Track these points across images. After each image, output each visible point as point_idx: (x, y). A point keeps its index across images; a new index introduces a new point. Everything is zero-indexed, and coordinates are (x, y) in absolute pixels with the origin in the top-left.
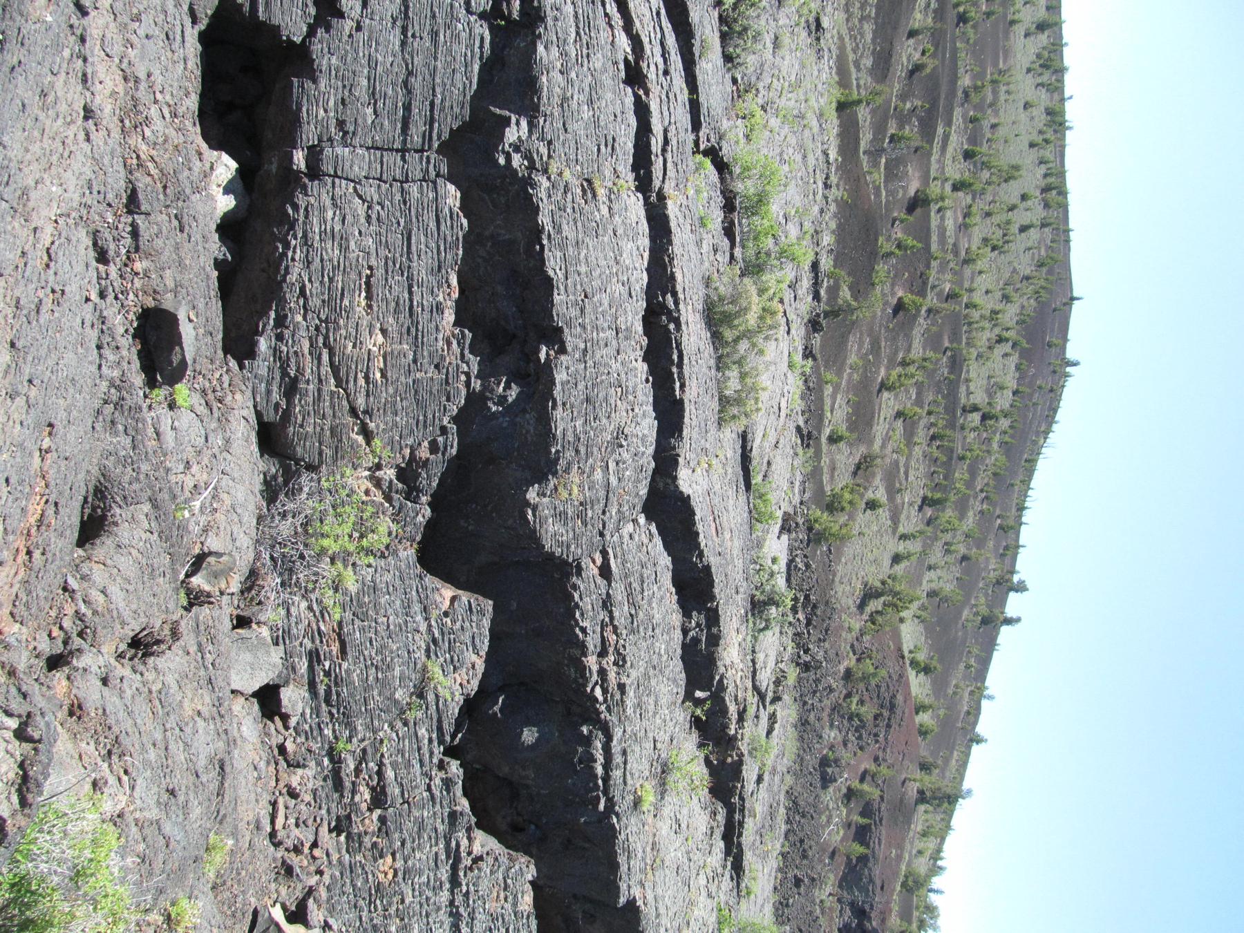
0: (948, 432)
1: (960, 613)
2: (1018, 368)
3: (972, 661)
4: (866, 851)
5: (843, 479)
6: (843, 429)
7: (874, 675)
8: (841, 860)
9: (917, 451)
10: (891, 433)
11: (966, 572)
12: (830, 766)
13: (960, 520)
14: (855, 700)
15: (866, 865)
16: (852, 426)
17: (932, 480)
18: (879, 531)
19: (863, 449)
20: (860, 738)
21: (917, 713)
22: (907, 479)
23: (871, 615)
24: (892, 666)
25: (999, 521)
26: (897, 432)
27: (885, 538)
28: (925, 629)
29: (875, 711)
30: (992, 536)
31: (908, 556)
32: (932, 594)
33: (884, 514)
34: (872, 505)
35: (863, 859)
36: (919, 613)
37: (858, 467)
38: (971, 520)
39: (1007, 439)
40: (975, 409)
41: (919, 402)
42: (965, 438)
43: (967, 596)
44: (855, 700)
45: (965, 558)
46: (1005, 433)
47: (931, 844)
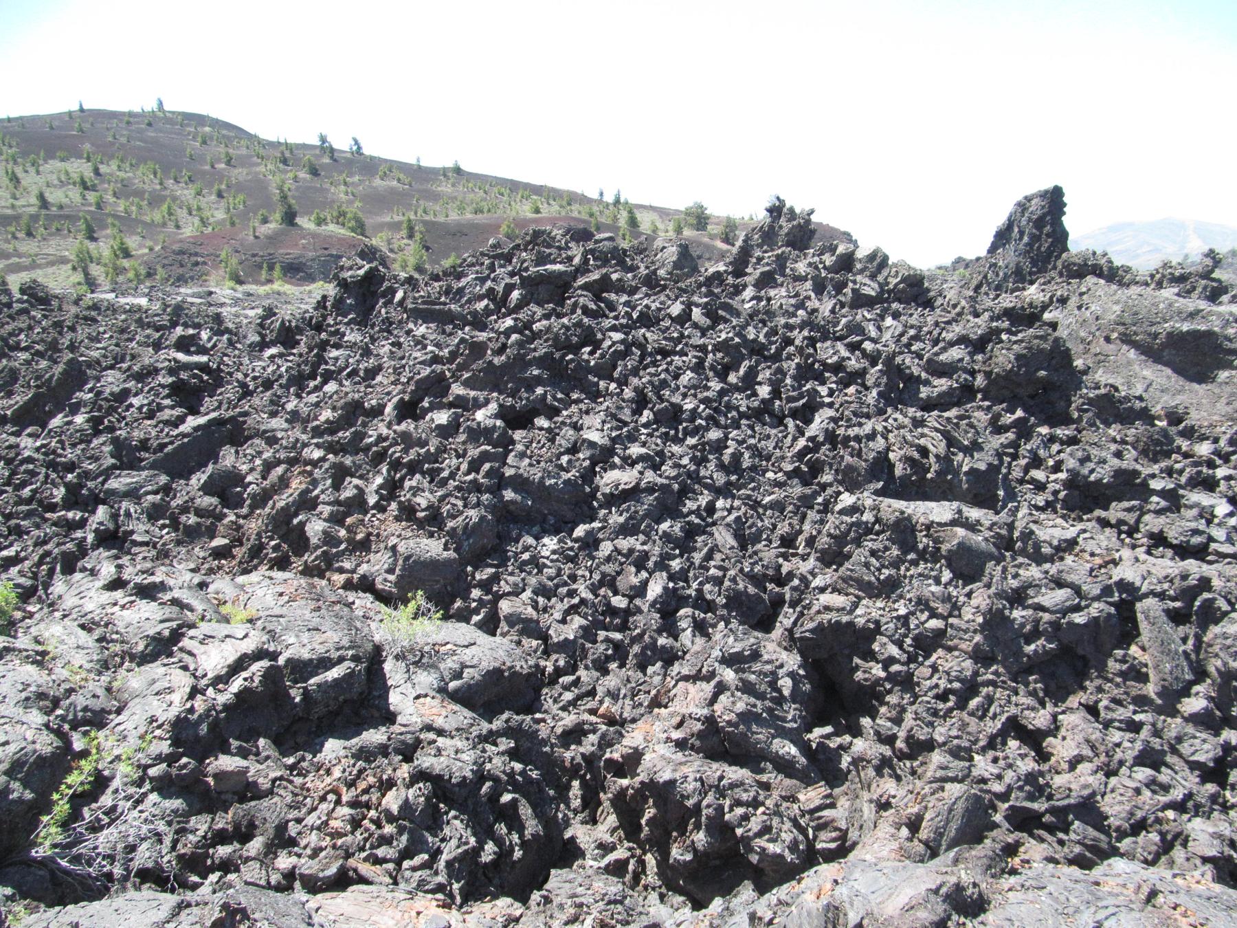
2: (62, 160)
38: (186, 192)
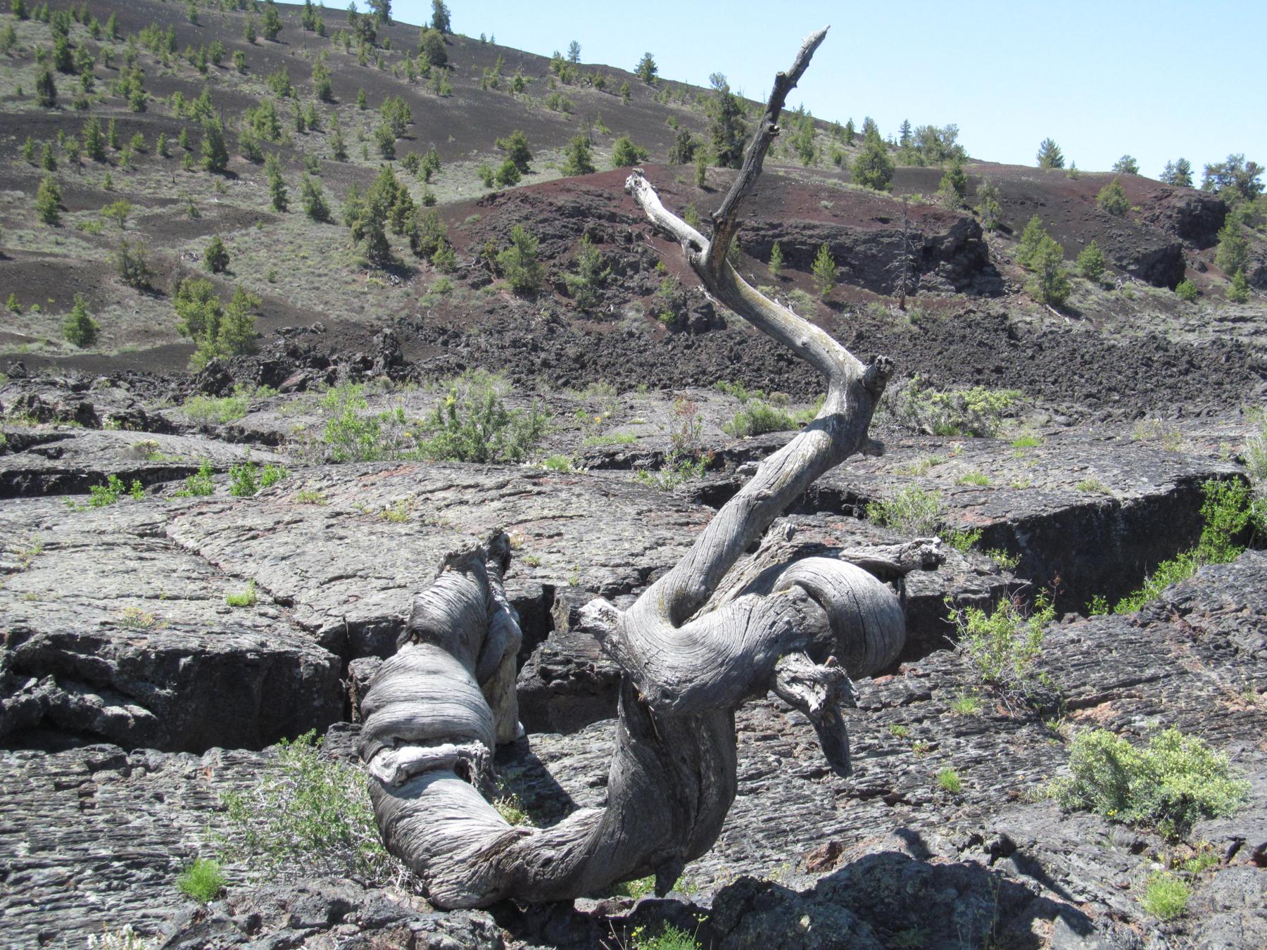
0: (88, 131)
1: (424, 102)
3: (511, 80)
4: (825, 250)
5: (171, 316)
6: (68, 319)
7: (523, 246)
8: (844, 292)
9: (123, 184)
10: (86, 232)
11: (350, 91)
12: (686, 317)
13: (254, 104)
14: (569, 277)
15: (850, 250)
16: (64, 302)
17: (180, 156)
18: (268, 247)
19: (113, 282)
20: (635, 267)
21: (592, 170)
22: (174, 202)
23: (419, 255)
24: (506, 216)
25: (261, 40)
26: (86, 221)
27: (282, 235)
28: (450, 160)
29: (584, 241)
30: (287, 52)
31: (313, 194)
32: (389, 151)
33: (234, 241)
34: (218, 261)
35: (840, 255)
36: (421, 172)
37: (146, 289)
38: (257, 88)
39: (108, 29)
40: (47, 85)
41: (29, 185)
42: (103, 102)
43: (396, 90)
44: (569, 277)
45: (326, 96)
46: (96, 32)
47: (825, 143)
